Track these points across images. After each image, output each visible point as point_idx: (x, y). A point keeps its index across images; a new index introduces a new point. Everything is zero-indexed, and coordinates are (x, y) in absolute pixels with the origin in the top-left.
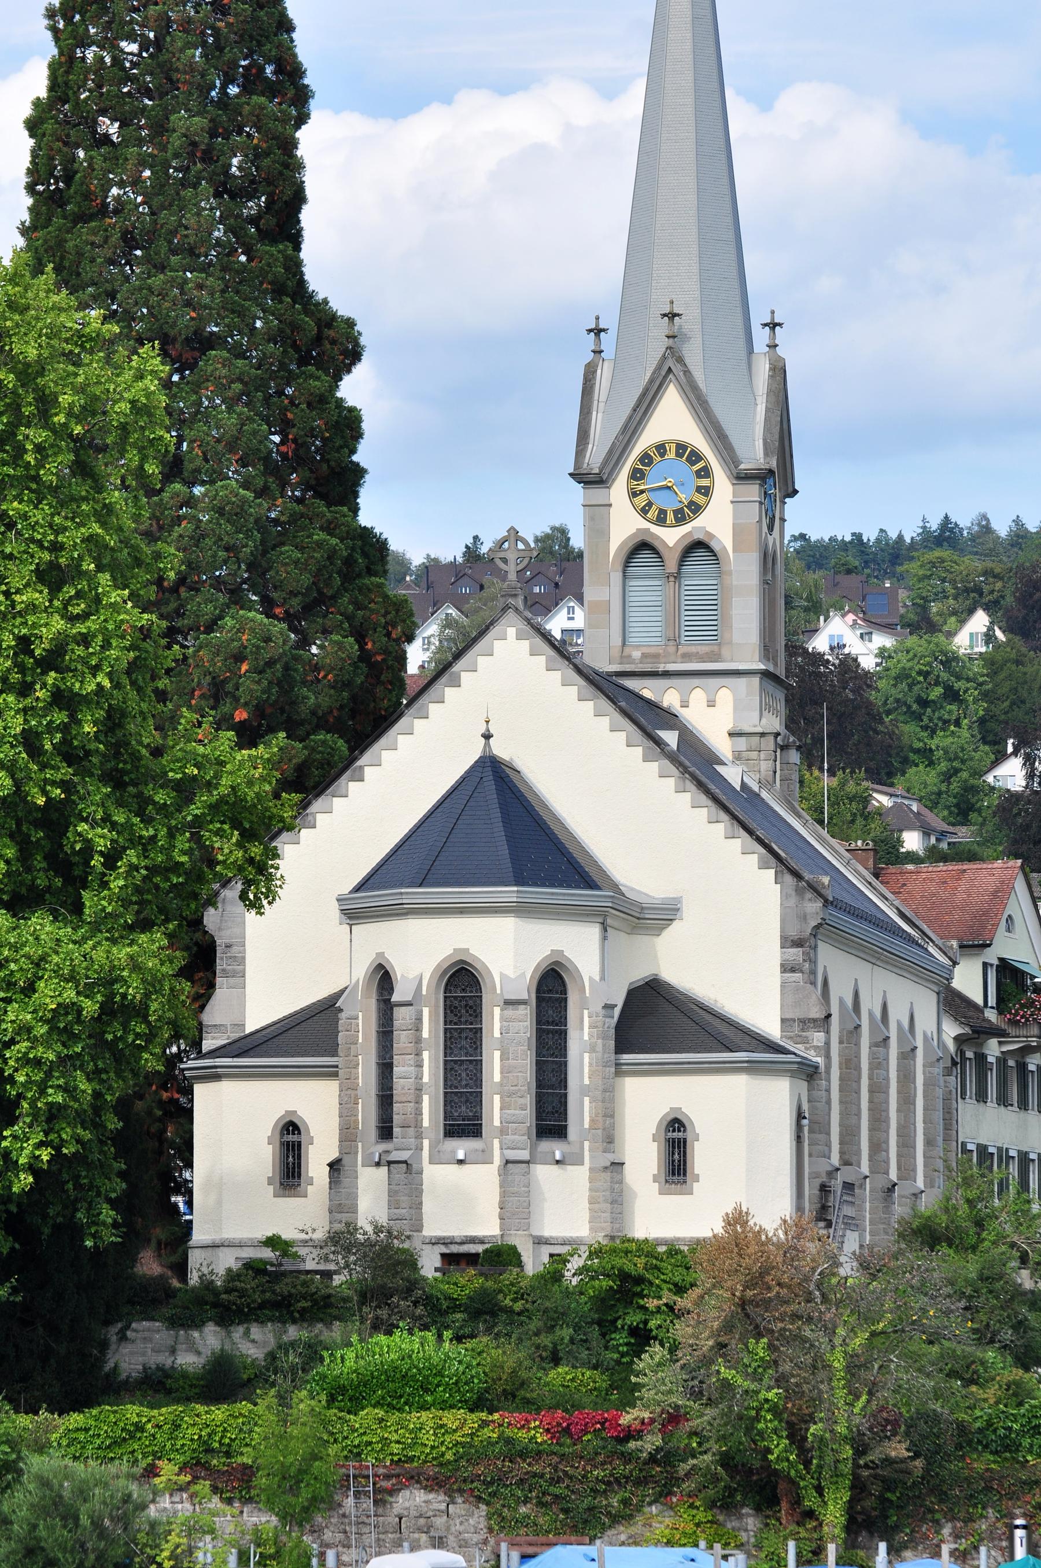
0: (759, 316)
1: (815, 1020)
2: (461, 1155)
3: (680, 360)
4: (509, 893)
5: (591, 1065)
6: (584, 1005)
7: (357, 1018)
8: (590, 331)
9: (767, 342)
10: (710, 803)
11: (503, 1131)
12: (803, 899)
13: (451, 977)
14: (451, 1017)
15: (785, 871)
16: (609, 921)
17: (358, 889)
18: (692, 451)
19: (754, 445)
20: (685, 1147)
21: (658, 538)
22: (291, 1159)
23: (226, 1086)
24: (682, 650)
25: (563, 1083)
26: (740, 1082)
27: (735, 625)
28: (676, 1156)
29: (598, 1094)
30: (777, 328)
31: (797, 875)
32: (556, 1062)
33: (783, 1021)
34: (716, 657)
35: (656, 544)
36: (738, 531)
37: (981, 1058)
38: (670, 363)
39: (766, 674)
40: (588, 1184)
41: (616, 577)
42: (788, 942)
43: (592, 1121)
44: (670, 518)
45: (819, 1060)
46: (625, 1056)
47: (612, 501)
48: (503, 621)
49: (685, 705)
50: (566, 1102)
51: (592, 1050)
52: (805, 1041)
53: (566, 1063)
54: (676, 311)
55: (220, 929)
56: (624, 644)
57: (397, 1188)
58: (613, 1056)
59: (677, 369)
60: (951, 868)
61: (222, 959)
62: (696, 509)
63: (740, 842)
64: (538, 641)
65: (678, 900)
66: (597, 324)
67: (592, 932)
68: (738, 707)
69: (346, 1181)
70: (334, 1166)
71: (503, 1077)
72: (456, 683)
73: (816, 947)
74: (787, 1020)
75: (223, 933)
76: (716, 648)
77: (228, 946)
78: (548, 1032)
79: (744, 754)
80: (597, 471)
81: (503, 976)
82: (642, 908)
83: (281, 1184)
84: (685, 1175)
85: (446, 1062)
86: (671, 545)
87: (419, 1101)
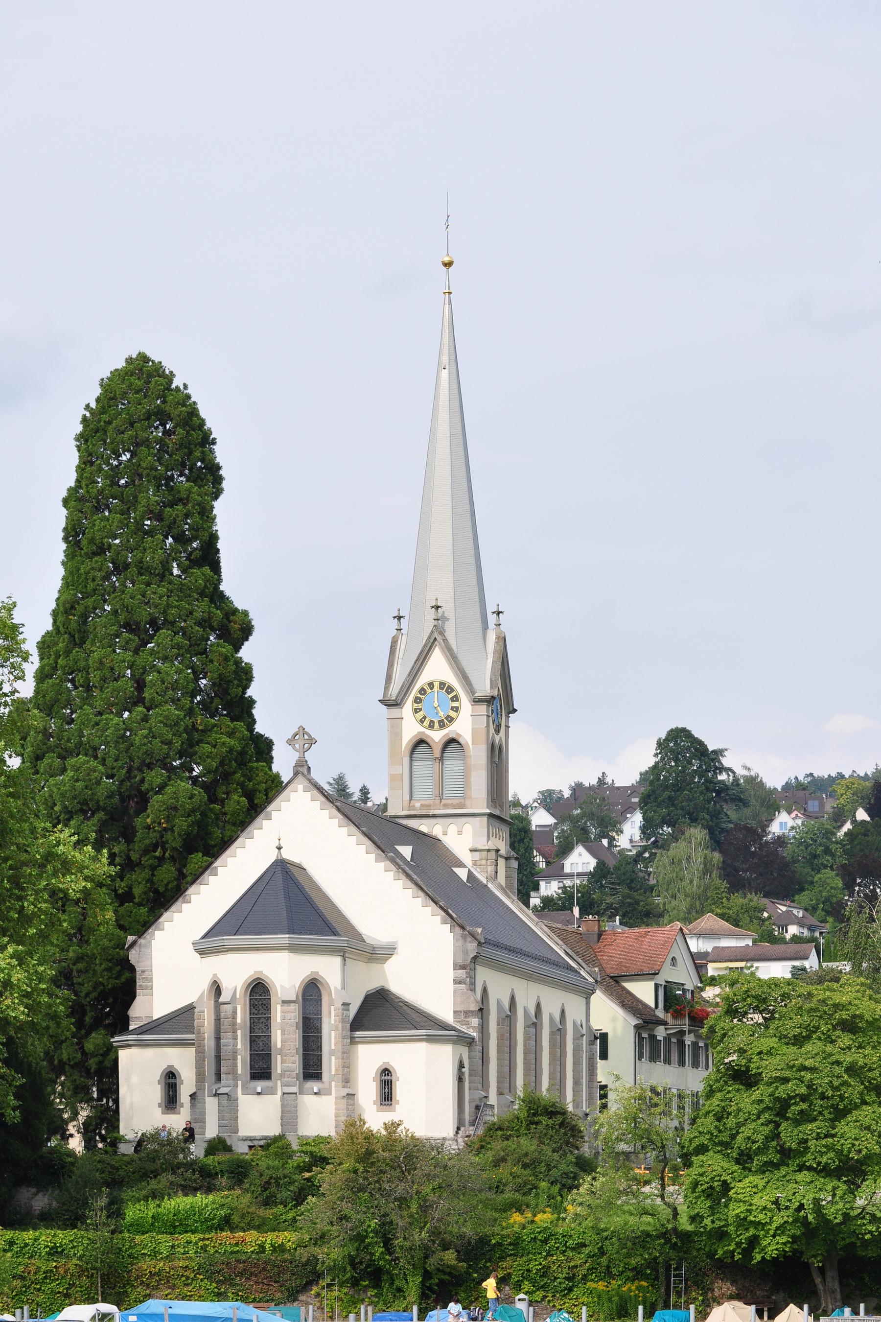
0: (491, 608)
1: (472, 1012)
2: (259, 1090)
3: (442, 633)
4: (284, 939)
5: (335, 1038)
6: (331, 1004)
7: (204, 1012)
8: (395, 617)
9: (495, 622)
10: (413, 886)
12: (466, 941)
13: (253, 987)
14: (254, 1011)
15: (456, 925)
16: (347, 955)
17: (203, 937)
18: (449, 686)
19: (485, 682)
20: (391, 1085)
21: (429, 737)
22: (171, 1093)
23: (134, 1050)
24: (443, 802)
25: (320, 1048)
26: (423, 1045)
27: (473, 787)
28: (387, 1090)
29: (340, 1054)
30: (501, 614)
31: (462, 927)
32: (315, 1036)
33: (455, 1012)
34: (462, 806)
35: (428, 740)
36: (474, 732)
37: (653, 1038)
38: (436, 635)
39: (491, 816)
40: (334, 1107)
41: (406, 760)
42: (457, 966)
43: (336, 1070)
44: (436, 725)
45: (475, 1034)
46: (358, 1033)
47: (403, 716)
49: (445, 833)
50: (321, 1059)
51: (336, 1029)
52: (467, 1023)
53: (321, 1037)
54: (439, 605)
55: (138, 962)
56: (411, 799)
57: (223, 1108)
58: (349, 1033)
59: (439, 638)
60: (641, 930)
61: (139, 979)
62: (451, 719)
63: (431, 908)
64: (316, 792)
65: (396, 943)
66: (399, 613)
67: (337, 960)
68: (475, 835)
69: (198, 1105)
70: (193, 1096)
72: (269, 818)
73: (475, 969)
74: (457, 1011)
75: (140, 964)
76: (462, 801)
77: (143, 972)
79: (478, 862)
80: (394, 698)
82: (374, 948)
83: (166, 1107)
84: (391, 1100)
85: (251, 1036)
86: (437, 741)
87: (235, 1059)
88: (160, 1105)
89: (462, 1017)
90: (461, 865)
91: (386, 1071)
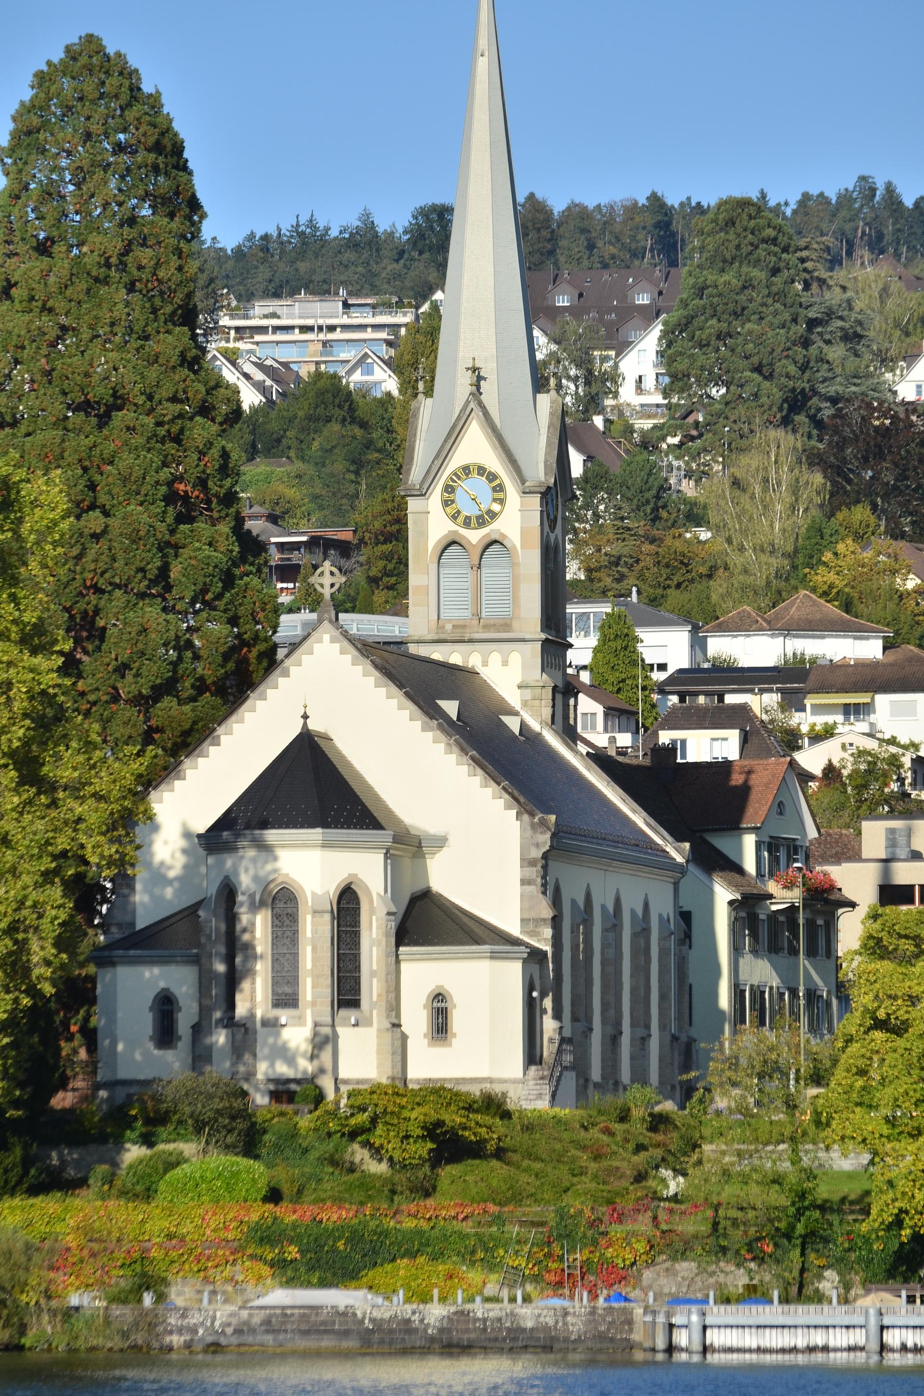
1: (544, 920)
6: (372, 911)
11: (314, 1004)
14: (277, 922)
25: (358, 968)
33: (522, 920)
36: (524, 533)
38: (472, 405)
41: (433, 567)
42: (527, 862)
43: (379, 995)
44: (474, 522)
48: (320, 629)
49: (485, 664)
51: (379, 945)
62: (493, 515)
71: (313, 966)
78: (347, 932)
81: (314, 894)
86: (474, 542)
88: (151, 1038)
89: (531, 927)
90: (514, 713)
91: (439, 997)
